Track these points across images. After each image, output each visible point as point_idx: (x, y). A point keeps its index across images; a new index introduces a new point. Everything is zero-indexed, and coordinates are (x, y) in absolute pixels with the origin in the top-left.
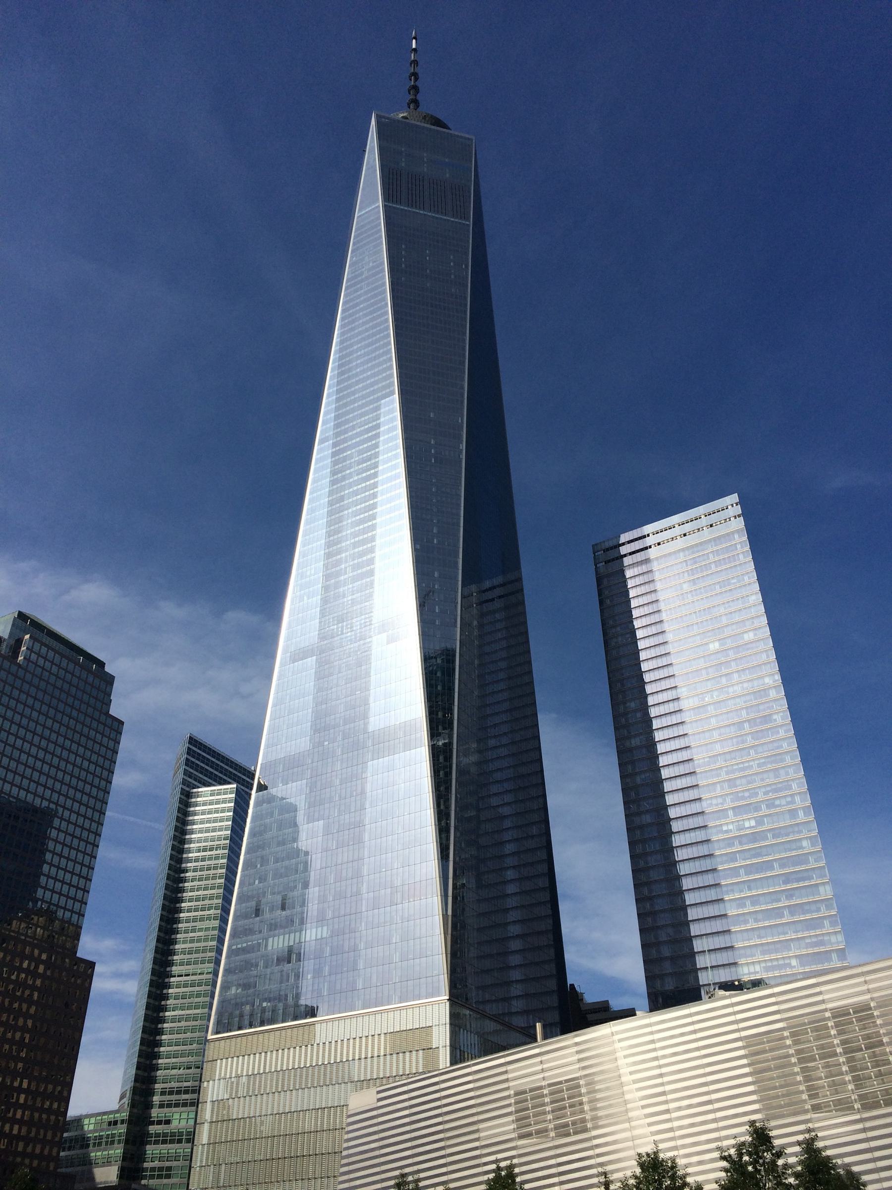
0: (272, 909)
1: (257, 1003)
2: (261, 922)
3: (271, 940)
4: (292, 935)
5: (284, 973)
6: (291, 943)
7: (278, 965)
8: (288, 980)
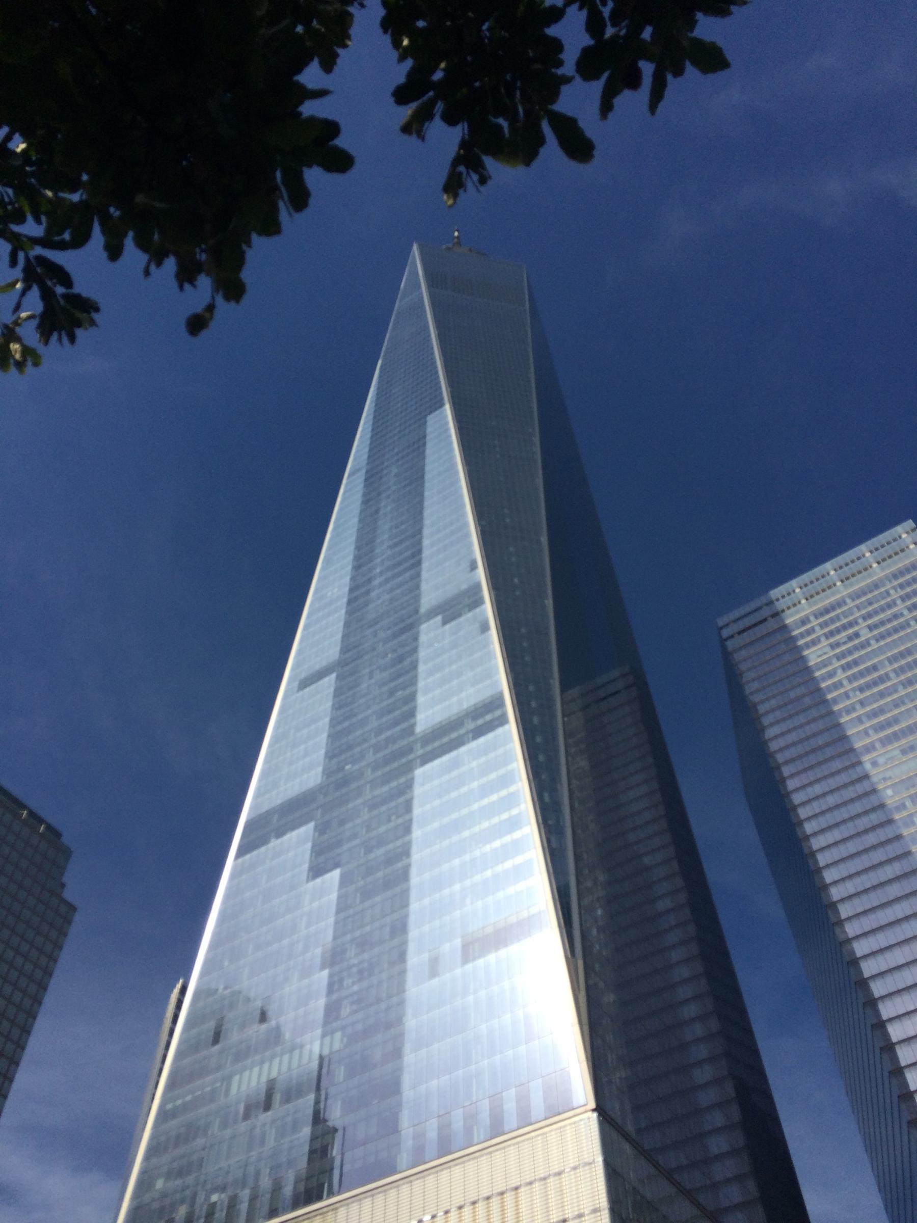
0: (243, 1026)
1: (201, 1198)
2: (221, 1052)
3: (236, 1078)
4: (276, 1061)
5: (257, 1131)
6: (274, 1074)
7: (246, 1116)
8: (262, 1142)
